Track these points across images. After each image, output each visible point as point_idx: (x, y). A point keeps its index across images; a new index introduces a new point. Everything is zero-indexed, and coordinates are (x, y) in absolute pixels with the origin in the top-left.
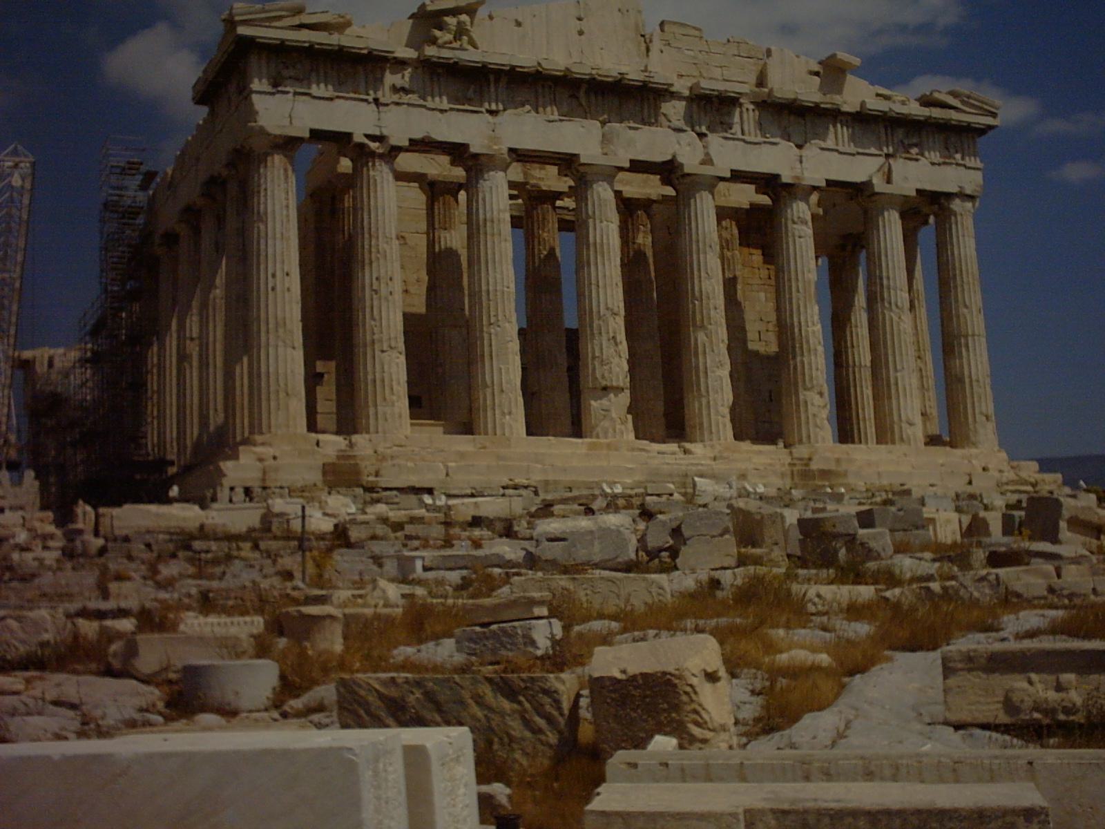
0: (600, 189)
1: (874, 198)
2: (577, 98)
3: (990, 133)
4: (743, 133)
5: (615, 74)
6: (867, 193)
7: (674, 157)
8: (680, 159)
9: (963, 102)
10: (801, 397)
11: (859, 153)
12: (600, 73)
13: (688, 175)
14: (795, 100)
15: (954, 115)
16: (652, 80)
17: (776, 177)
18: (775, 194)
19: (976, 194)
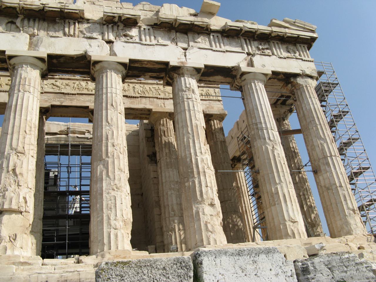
0: (23, 72)
1: (243, 78)
2: (15, 23)
3: (315, 45)
4: (141, 40)
5: (39, 4)
6: (238, 76)
7: (86, 52)
8: (90, 53)
9: (291, 24)
10: (194, 209)
11: (227, 51)
12: (26, 3)
13: (97, 62)
14: (176, 20)
15: (287, 30)
16: (66, 7)
17: (167, 64)
18: (169, 77)
19: (313, 75)
